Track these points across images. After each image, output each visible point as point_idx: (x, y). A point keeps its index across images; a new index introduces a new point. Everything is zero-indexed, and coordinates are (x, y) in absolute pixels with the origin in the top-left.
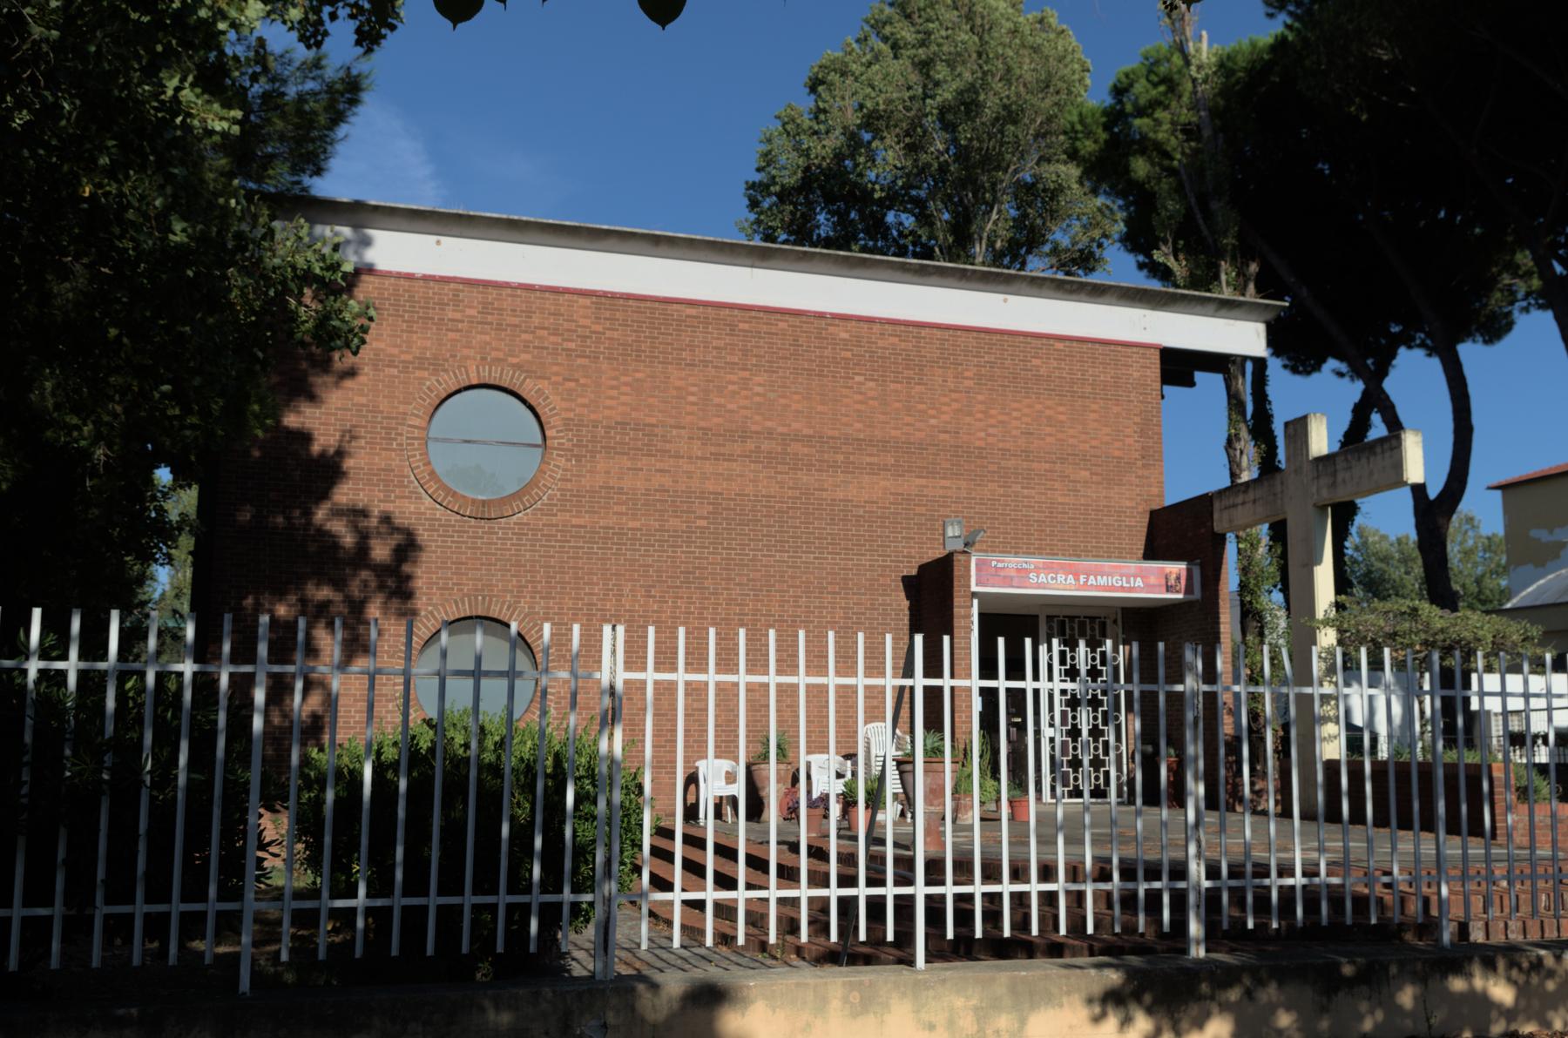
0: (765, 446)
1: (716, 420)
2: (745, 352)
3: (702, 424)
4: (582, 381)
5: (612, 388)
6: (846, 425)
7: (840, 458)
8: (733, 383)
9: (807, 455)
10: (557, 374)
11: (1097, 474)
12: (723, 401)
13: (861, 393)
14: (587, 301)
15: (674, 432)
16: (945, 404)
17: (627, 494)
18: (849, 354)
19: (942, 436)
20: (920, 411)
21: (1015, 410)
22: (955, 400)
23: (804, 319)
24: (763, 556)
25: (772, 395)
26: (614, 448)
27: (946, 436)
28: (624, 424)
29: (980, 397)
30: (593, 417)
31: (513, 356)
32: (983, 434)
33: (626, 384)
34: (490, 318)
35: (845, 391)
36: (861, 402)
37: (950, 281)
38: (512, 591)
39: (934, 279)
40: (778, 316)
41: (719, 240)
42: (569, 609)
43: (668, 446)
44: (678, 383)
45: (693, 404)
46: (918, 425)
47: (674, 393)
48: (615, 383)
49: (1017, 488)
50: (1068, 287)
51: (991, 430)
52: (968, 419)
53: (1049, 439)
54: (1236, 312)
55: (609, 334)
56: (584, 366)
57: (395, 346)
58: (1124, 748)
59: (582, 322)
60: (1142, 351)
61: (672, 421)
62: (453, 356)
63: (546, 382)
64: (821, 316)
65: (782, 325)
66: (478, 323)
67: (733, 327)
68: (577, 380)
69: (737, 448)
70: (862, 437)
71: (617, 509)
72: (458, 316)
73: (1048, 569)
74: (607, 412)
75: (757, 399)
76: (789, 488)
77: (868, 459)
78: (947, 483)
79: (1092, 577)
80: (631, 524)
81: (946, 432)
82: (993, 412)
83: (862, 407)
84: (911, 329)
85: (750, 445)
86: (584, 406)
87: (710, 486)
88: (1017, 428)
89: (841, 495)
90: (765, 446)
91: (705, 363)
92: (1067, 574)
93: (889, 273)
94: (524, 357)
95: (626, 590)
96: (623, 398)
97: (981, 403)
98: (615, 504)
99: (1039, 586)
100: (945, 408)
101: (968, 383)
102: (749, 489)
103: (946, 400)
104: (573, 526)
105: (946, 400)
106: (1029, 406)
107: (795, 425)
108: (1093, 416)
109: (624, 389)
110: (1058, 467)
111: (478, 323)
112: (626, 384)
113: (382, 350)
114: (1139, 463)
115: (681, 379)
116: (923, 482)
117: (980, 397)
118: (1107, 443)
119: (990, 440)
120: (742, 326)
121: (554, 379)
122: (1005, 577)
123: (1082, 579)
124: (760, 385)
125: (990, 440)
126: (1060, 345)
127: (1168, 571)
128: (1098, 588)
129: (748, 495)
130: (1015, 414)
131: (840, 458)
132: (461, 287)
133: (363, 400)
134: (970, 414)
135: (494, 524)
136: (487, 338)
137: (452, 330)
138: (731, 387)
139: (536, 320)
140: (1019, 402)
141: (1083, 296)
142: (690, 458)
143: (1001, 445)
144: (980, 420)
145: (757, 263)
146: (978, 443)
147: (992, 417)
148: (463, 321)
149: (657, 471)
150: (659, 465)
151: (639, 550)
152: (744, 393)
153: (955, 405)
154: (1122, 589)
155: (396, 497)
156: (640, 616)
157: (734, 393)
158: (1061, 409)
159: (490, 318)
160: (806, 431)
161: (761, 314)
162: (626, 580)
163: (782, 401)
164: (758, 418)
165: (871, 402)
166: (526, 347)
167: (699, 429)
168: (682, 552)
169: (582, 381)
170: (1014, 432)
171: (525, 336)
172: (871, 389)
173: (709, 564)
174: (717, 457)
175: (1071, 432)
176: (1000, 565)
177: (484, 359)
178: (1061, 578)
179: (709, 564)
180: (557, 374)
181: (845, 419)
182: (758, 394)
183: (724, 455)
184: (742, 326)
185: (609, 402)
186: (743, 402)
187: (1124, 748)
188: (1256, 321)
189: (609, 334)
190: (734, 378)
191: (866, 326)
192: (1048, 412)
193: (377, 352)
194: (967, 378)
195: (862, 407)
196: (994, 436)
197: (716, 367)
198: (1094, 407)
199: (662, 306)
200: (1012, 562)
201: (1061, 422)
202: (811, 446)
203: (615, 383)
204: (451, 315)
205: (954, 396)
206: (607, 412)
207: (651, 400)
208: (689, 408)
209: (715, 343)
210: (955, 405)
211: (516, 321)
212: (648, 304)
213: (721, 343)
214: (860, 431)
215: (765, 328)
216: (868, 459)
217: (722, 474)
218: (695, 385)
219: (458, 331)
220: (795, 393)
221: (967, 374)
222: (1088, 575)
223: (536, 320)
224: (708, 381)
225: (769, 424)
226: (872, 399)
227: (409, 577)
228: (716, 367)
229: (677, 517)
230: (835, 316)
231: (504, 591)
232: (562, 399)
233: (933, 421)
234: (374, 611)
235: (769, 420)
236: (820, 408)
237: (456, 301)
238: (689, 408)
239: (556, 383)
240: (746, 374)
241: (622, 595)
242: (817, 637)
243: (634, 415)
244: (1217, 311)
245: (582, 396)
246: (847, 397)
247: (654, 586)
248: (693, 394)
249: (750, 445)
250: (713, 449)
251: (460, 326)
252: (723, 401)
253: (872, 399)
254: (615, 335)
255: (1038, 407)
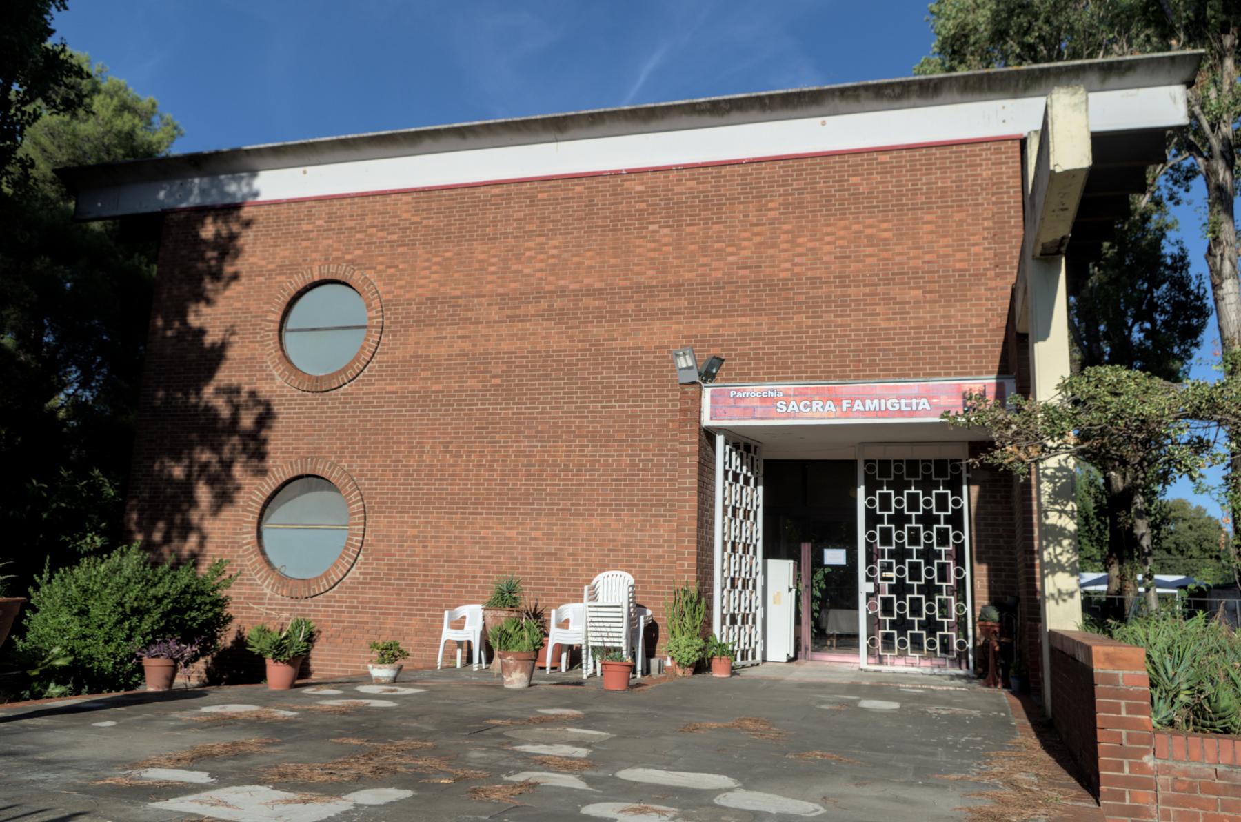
0: (558, 303)
1: (513, 285)
2: (543, 220)
3: (501, 290)
4: (401, 267)
5: (425, 269)
6: (638, 274)
7: (632, 306)
8: (530, 249)
9: (597, 308)
10: (381, 264)
11: (931, 292)
12: (520, 267)
13: (654, 241)
14: (407, 198)
15: (476, 301)
16: (745, 239)
17: (433, 360)
18: (643, 205)
19: (741, 272)
20: (718, 250)
21: (828, 234)
22: (758, 234)
23: (600, 179)
24: (551, 408)
25: (565, 255)
26: (424, 321)
27: (747, 272)
28: (432, 299)
29: (786, 227)
30: (408, 296)
31: (348, 253)
32: (788, 265)
33: (436, 264)
34: (333, 225)
35: (638, 242)
36: (654, 250)
37: (754, 114)
38: (336, 453)
39: (735, 115)
40: (576, 181)
41: (510, 120)
42: (379, 466)
43: (469, 314)
44: (482, 257)
45: (493, 273)
46: (714, 264)
47: (477, 266)
48: (427, 264)
49: (831, 317)
50: (888, 91)
51: (796, 260)
52: (771, 252)
53: (869, 261)
54: (1130, 78)
55: (425, 222)
56: (403, 254)
57: (264, 259)
58: (969, 609)
59: (405, 216)
60: (994, 146)
61: (473, 291)
62: (304, 260)
63: (373, 271)
64: (617, 173)
65: (578, 189)
66: (325, 230)
67: (532, 198)
68: (397, 267)
69: (531, 309)
70: (654, 283)
71: (423, 374)
72: (310, 227)
73: (800, 396)
74: (419, 291)
75: (552, 261)
76: (579, 341)
77: (660, 305)
78: (742, 320)
79: (858, 402)
80: (435, 387)
81: (746, 268)
82: (800, 240)
83: (656, 255)
84: (710, 169)
85: (544, 305)
86: (401, 287)
87: (505, 347)
88: (830, 253)
89: (630, 343)
90: (558, 303)
91: (506, 235)
92: (825, 400)
93: (685, 120)
94: (358, 252)
95: (427, 448)
96: (434, 277)
97: (787, 232)
98: (422, 370)
99: (788, 415)
100: (745, 244)
101: (771, 214)
102: (541, 346)
103: (747, 234)
104: (387, 393)
105: (747, 234)
106: (845, 228)
107: (587, 281)
108: (927, 228)
109: (435, 268)
110: (880, 289)
111: (325, 230)
112: (436, 264)
113: (255, 263)
114: (991, 274)
115: (484, 252)
116: (720, 321)
117: (786, 227)
118: (947, 256)
119: (797, 270)
120: (540, 196)
121: (379, 268)
122: (746, 408)
123: (845, 404)
124: (555, 247)
125: (797, 270)
126: (885, 158)
127: (966, 388)
128: (866, 413)
129: (540, 352)
130: (827, 239)
131: (632, 306)
132: (314, 203)
133: (239, 305)
134: (774, 246)
135: (326, 396)
136: (330, 242)
137: (305, 240)
138: (528, 254)
139: (368, 221)
140: (834, 225)
141: (914, 100)
142: (488, 322)
143: (810, 274)
144: (786, 250)
145: (559, 136)
146: (782, 275)
147: (799, 245)
148: (312, 231)
149: (459, 337)
150: (461, 332)
151: (440, 410)
152: (540, 257)
153: (757, 239)
154: (900, 413)
155: (258, 380)
156: (438, 470)
157: (531, 258)
158: (884, 226)
159: (333, 225)
160: (598, 285)
161: (560, 182)
162: (428, 438)
163: (576, 259)
164: (551, 278)
165: (664, 249)
166: (359, 244)
167: (497, 295)
168: (477, 410)
169: (401, 267)
170: (825, 258)
171: (359, 236)
172: (666, 236)
173: (501, 419)
174: (512, 318)
175: (898, 249)
176: (740, 395)
177: (326, 259)
178: (817, 405)
179: (501, 419)
180: (381, 264)
181: (637, 269)
182: (553, 256)
183: (519, 316)
184: (540, 196)
185: (422, 282)
186: (539, 266)
187: (969, 609)
188: (1170, 84)
189: (425, 222)
190: (531, 244)
191: (661, 175)
192: (869, 231)
193: (251, 265)
194: (771, 209)
195: (656, 255)
196: (801, 265)
197: (515, 237)
198: (927, 218)
199: (471, 191)
200: (754, 391)
201: (885, 239)
202: (601, 299)
203: (427, 264)
204: (305, 227)
205: (756, 229)
206: (419, 291)
207: (456, 275)
208: (490, 278)
209: (516, 215)
210: (757, 239)
211: (352, 224)
212: (459, 191)
213: (521, 215)
214: (651, 278)
215: (562, 194)
216: (660, 305)
217: (516, 335)
218: (494, 256)
219: (309, 239)
220: (589, 250)
221: (771, 205)
222: (853, 400)
223: (368, 221)
224: (507, 251)
225: (562, 283)
226: (666, 245)
227: (264, 442)
228: (515, 237)
229: (475, 377)
230: (631, 172)
231: (330, 452)
232: (384, 284)
233: (731, 259)
234: (237, 470)
235: (563, 279)
236: (612, 261)
237: (310, 215)
238: (490, 278)
239: (380, 271)
240: (543, 239)
241: (423, 452)
242: (602, 485)
243: (442, 289)
244: (1103, 81)
245: (401, 279)
246: (639, 246)
247: (451, 442)
248: (493, 265)
249: (544, 305)
250: (509, 312)
251: (311, 235)
252: (520, 267)
253: (666, 245)
254: (430, 222)
255: (855, 227)
